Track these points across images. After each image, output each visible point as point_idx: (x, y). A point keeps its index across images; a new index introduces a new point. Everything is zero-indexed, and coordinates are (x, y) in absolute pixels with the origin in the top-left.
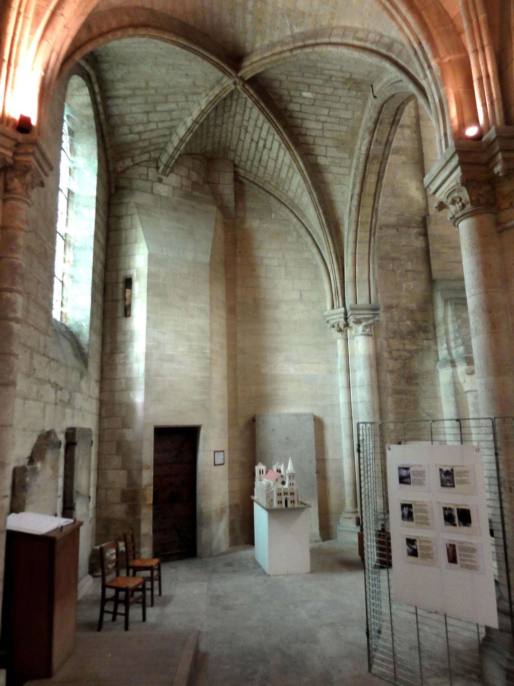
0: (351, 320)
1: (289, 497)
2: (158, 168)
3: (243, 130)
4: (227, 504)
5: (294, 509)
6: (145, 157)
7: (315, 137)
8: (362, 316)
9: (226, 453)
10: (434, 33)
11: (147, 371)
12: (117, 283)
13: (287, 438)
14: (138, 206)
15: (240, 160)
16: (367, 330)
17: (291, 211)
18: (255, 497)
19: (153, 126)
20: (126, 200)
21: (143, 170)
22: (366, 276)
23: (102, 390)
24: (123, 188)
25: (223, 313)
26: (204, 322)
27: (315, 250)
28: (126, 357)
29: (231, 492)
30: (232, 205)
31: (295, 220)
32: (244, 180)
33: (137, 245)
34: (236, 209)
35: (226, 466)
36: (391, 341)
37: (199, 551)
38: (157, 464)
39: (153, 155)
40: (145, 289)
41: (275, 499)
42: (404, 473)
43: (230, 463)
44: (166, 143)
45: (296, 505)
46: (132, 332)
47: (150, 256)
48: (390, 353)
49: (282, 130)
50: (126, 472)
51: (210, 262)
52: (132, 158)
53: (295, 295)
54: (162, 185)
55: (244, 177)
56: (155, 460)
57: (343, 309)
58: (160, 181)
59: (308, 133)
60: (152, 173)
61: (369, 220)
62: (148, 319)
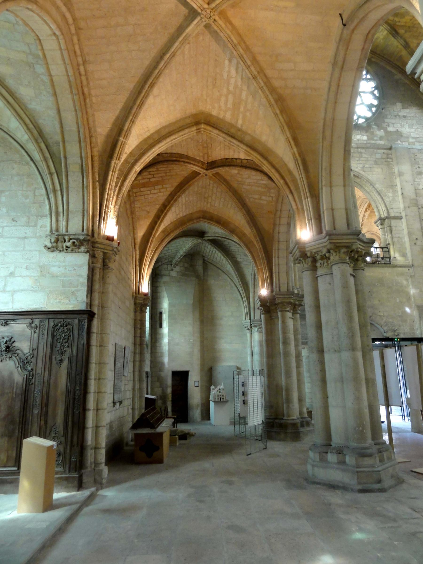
0: (252, 325)
1: (222, 397)
5: (223, 402)
7: (235, 252)
8: (257, 324)
9: (200, 382)
10: (256, 259)
12: (157, 314)
13: (225, 376)
14: (164, 283)
17: (228, 276)
18: (211, 399)
19: (170, 251)
21: (165, 266)
23: (151, 357)
24: (158, 275)
25: (198, 323)
26: (190, 329)
27: (238, 293)
28: (161, 344)
29: (201, 398)
30: (202, 275)
31: (229, 280)
32: (208, 263)
34: (204, 276)
35: (199, 387)
37: (189, 419)
38: (173, 386)
39: (170, 260)
40: (168, 317)
41: (217, 398)
42: (243, 384)
43: (202, 386)
44: (175, 255)
45: (224, 400)
47: (169, 303)
51: (193, 303)
52: (161, 262)
53: (230, 313)
54: (173, 272)
55: (207, 261)
58: (172, 270)
59: (232, 250)
60: (169, 267)
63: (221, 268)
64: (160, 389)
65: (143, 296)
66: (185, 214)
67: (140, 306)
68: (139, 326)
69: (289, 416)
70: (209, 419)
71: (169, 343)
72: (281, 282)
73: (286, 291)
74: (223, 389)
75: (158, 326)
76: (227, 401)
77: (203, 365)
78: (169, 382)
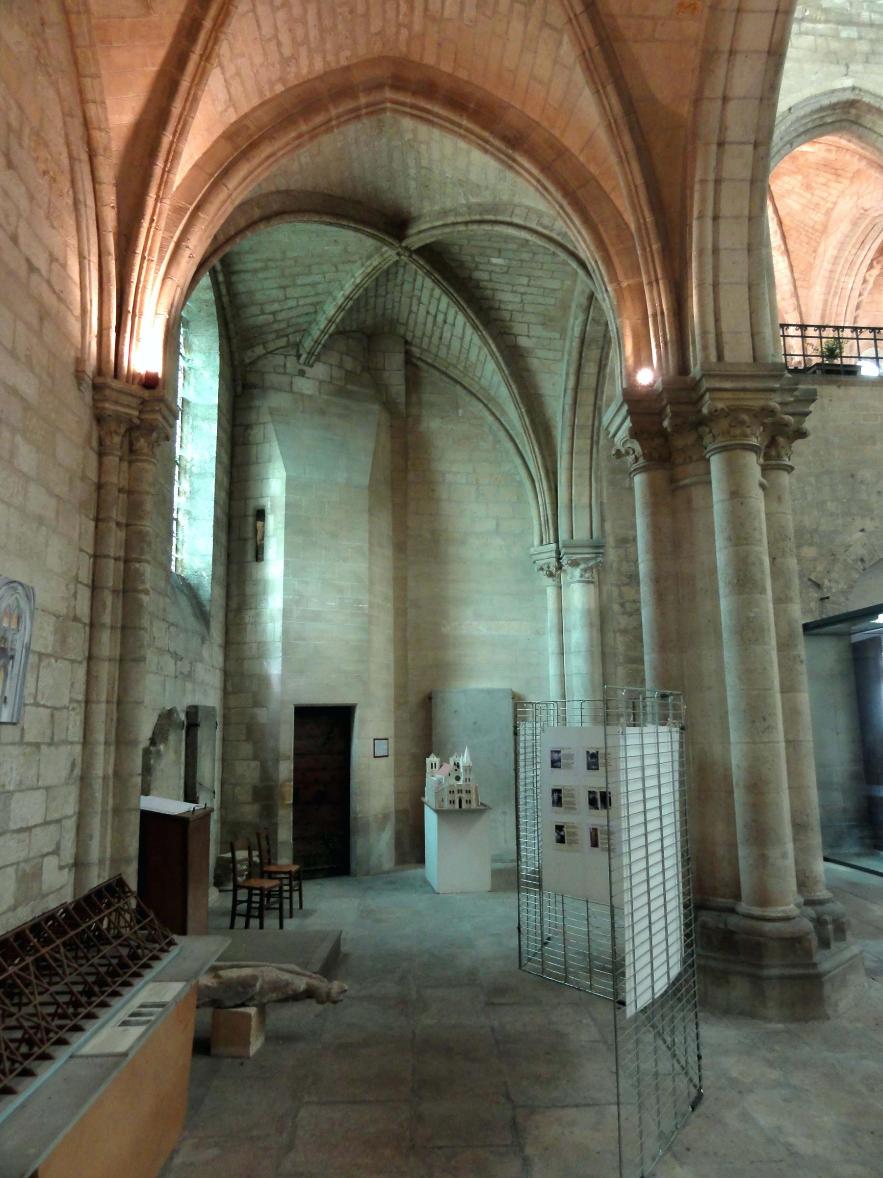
0: (564, 561)
1: (464, 796)
2: (299, 356)
3: (415, 301)
4: (392, 808)
6: (282, 342)
7: (512, 311)
8: (579, 556)
9: (391, 741)
10: (612, 251)
11: (285, 632)
12: (245, 516)
14: (272, 412)
15: (414, 336)
16: (587, 575)
17: (486, 406)
18: (426, 799)
19: (292, 303)
20: (257, 403)
21: (279, 360)
22: (586, 500)
23: (226, 658)
24: (254, 386)
25: (388, 552)
26: (361, 566)
27: (518, 461)
28: (258, 615)
29: (397, 794)
30: (402, 399)
31: (490, 419)
32: (419, 363)
33: (271, 466)
34: (408, 403)
35: (391, 758)
36: (624, 589)
37: (353, 866)
38: (298, 754)
39: (292, 338)
40: (282, 525)
41: (447, 798)
42: (556, 756)
43: (397, 754)
44: (310, 323)
45: (474, 805)
46: (265, 582)
48: (622, 605)
49: (465, 306)
50: (258, 763)
51: (370, 484)
52: (264, 344)
53: (490, 525)
54: (304, 380)
55: (420, 359)
56: (295, 749)
57: (554, 546)
58: (302, 373)
59: (502, 306)
60: (291, 364)
61: (590, 423)
62: (286, 564)
63: (466, 381)
64: (254, 764)
65: (135, 388)
66: (319, 66)
67: (122, 430)
68: (116, 513)
69: (764, 900)
70: (421, 860)
71: (286, 614)
72: (724, 327)
73: (751, 360)
74: (468, 769)
75: (250, 555)
76: (482, 810)
77: (401, 687)
78: (286, 740)
